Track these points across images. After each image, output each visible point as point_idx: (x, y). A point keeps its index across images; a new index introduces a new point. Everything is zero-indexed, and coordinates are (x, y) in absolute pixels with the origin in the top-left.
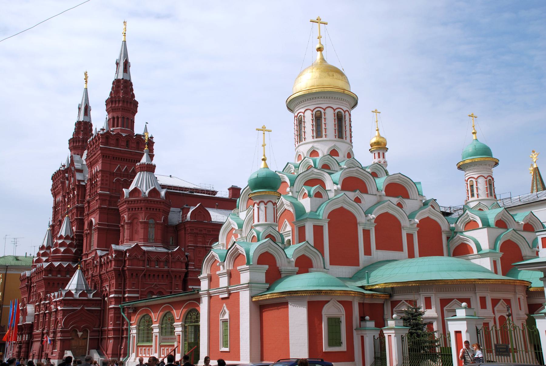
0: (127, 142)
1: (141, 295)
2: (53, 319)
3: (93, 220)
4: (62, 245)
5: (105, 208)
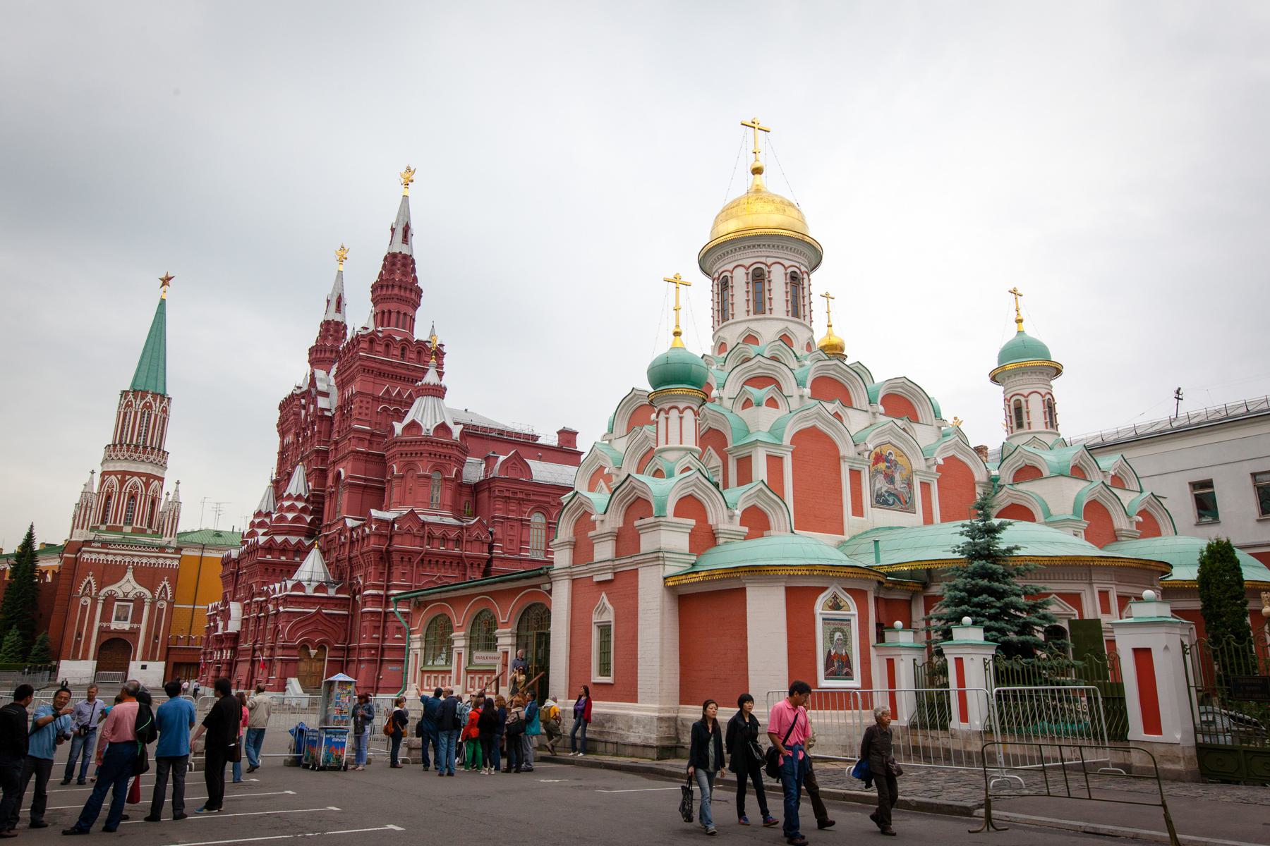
0: (403, 349)
2: (270, 626)
4: (291, 508)
5: (362, 453)
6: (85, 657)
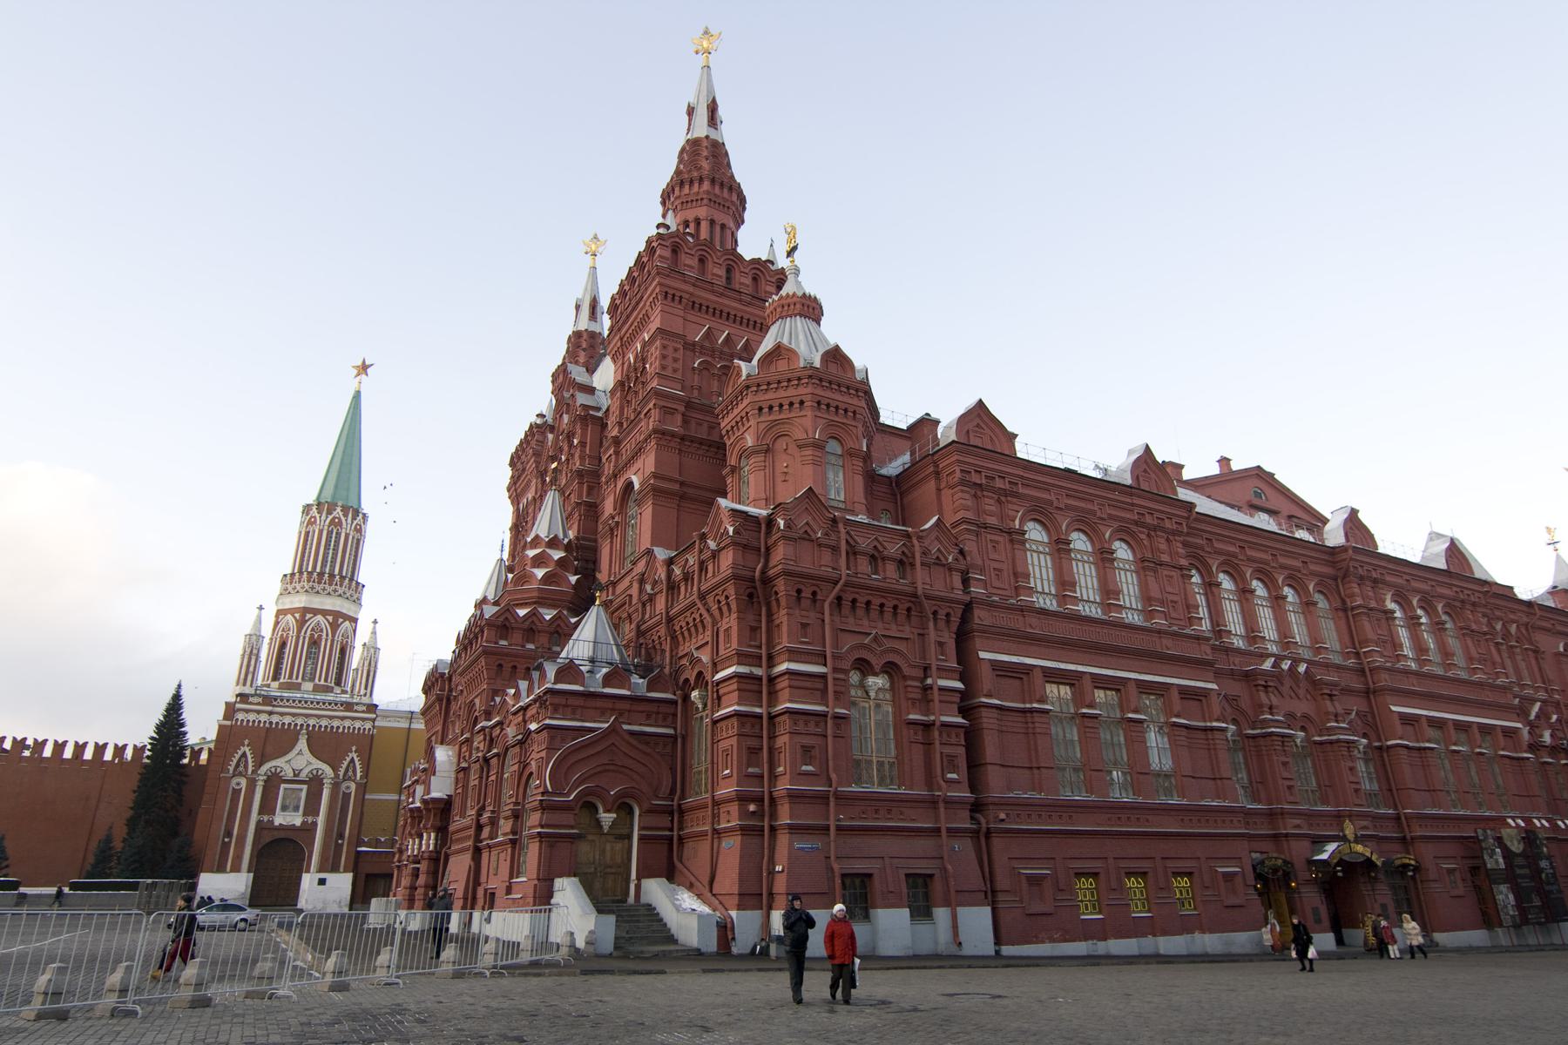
1: (835, 670)
2: (511, 768)
5: (673, 435)
6: (236, 869)
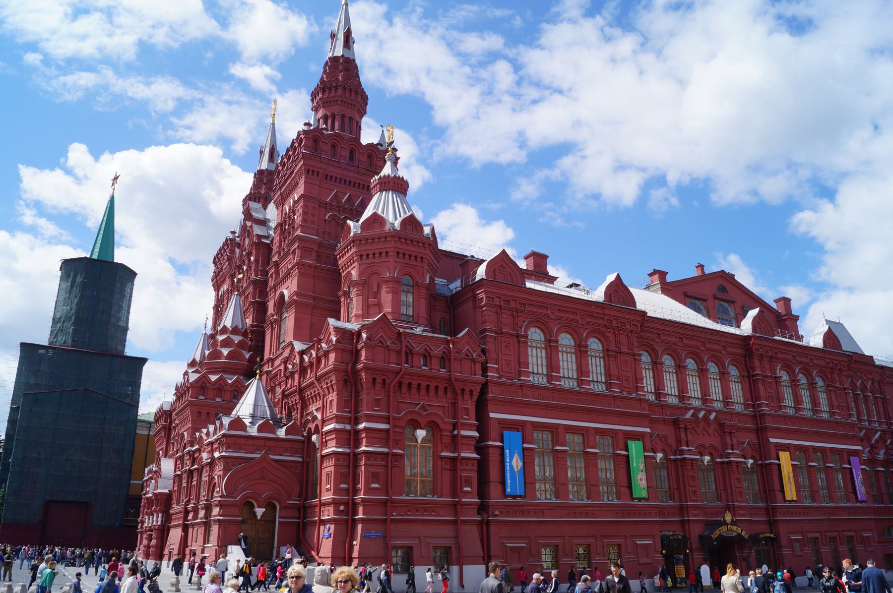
1: (394, 426)
3: (286, 292)
5: (310, 266)
